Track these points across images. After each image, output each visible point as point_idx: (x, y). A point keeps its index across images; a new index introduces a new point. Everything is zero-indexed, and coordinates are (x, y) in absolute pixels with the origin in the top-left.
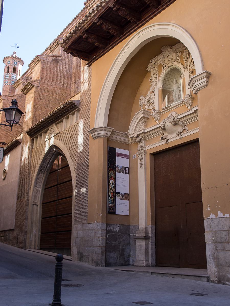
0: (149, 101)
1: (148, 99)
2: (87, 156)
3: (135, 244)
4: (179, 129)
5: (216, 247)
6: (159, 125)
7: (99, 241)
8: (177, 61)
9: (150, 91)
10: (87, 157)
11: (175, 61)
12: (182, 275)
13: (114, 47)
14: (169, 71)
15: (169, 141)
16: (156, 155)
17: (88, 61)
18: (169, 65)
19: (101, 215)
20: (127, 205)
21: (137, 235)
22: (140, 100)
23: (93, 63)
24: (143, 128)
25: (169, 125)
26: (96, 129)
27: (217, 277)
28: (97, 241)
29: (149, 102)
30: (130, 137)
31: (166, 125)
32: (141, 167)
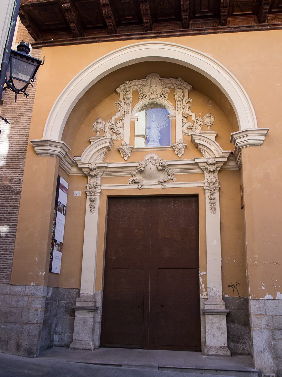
0: (113, 128)
1: (110, 126)
2: (18, 176)
3: (74, 316)
4: (163, 176)
5: (273, 335)
6: (137, 164)
7: (37, 315)
8: (165, 97)
9: (116, 117)
10: (15, 179)
11: (162, 96)
12: (216, 370)
13: (96, 43)
14: (149, 104)
15: (143, 187)
16: (114, 200)
17: (36, 40)
18: (152, 97)
19: (44, 274)
20: (60, 259)
21: (78, 304)
22: (95, 123)
23: (44, 48)
24: (100, 160)
25: (151, 168)
26: (49, 143)
27: (274, 373)
28: (34, 315)
29: (112, 130)
30: (80, 166)
31: (147, 168)
32: (92, 210)
